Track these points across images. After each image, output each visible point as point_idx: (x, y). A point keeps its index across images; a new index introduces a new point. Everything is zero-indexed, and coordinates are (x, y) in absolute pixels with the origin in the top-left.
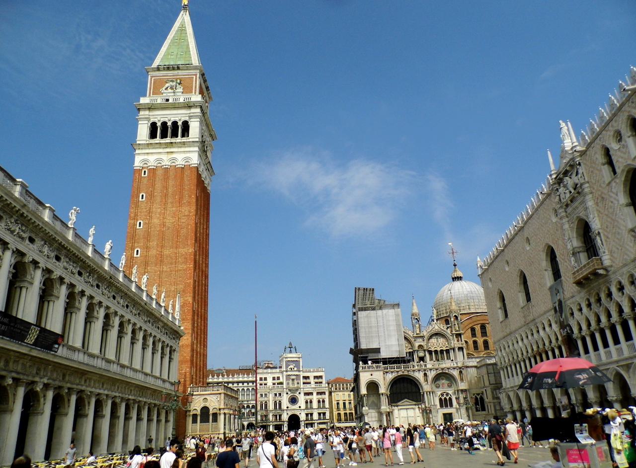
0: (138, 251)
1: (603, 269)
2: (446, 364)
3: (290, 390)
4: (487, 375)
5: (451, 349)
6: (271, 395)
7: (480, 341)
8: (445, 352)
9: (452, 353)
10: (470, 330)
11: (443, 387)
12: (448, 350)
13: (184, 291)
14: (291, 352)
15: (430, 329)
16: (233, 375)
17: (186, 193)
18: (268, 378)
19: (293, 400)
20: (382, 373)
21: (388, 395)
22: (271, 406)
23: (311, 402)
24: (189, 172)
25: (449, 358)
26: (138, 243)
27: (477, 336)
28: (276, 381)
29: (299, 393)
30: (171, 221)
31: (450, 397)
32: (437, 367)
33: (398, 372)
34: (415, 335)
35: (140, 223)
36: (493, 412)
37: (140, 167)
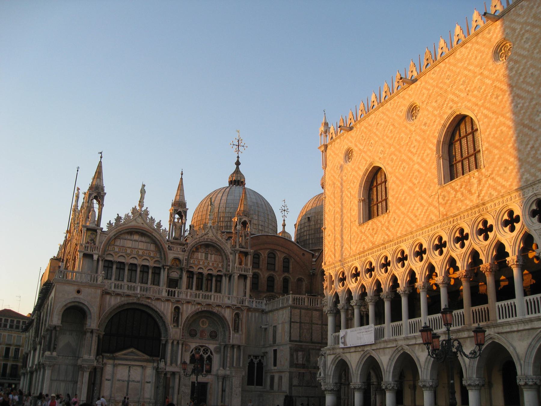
2: (214, 298)
4: (287, 326)
5: (225, 275)
7: (264, 275)
8: (214, 279)
9: (225, 281)
11: (202, 337)
12: (221, 276)
20: (99, 292)
21: (101, 336)
25: (218, 290)
27: (261, 267)
31: (209, 356)
32: (200, 300)
33: (128, 296)
36: (285, 387)
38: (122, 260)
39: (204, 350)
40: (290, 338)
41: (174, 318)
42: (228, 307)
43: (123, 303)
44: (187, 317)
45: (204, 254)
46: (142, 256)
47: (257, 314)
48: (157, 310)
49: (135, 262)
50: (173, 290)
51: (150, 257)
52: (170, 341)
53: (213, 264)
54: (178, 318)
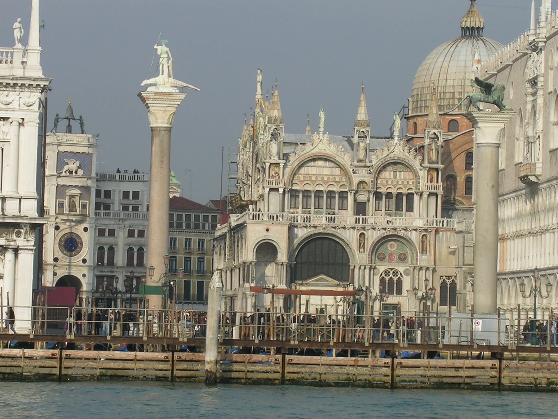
1: (535, 176)
2: (399, 222)
8: (405, 198)
9: (416, 198)
10: (463, 156)
12: (413, 194)
14: (69, 130)
15: (386, 153)
19: (70, 245)
21: (293, 266)
23: (111, 249)
25: (410, 208)
33: (315, 227)
34: (356, 163)
38: (307, 188)
39: (394, 272)
40: (464, 262)
41: (360, 244)
42: (416, 230)
43: (310, 234)
44: (373, 243)
45: (392, 172)
46: (328, 182)
47: (449, 233)
48: (343, 238)
49: (321, 188)
50: (358, 217)
51: (336, 182)
52: (357, 267)
53: (403, 182)
54: (364, 244)
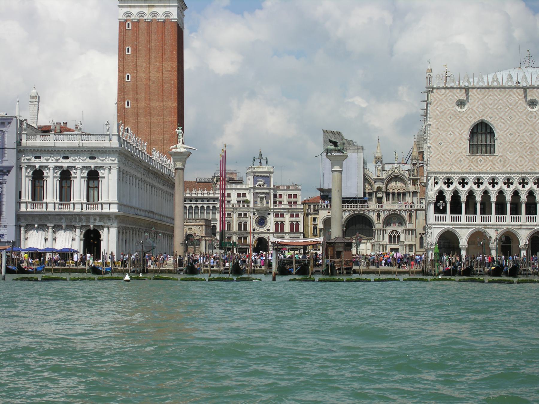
0: (128, 102)
3: (257, 210)
6: (235, 215)
13: (170, 140)
16: (191, 190)
17: (168, 48)
18: (232, 195)
22: (235, 227)
23: (282, 224)
24: (170, 26)
26: (128, 95)
28: (241, 199)
29: (269, 214)
30: (155, 76)
33: (354, 211)
34: (375, 178)
35: (128, 76)
37: (124, 20)
